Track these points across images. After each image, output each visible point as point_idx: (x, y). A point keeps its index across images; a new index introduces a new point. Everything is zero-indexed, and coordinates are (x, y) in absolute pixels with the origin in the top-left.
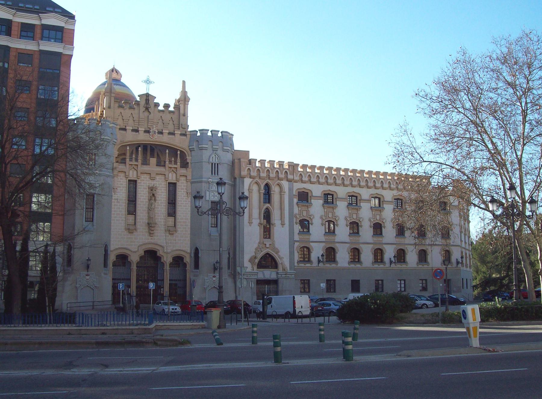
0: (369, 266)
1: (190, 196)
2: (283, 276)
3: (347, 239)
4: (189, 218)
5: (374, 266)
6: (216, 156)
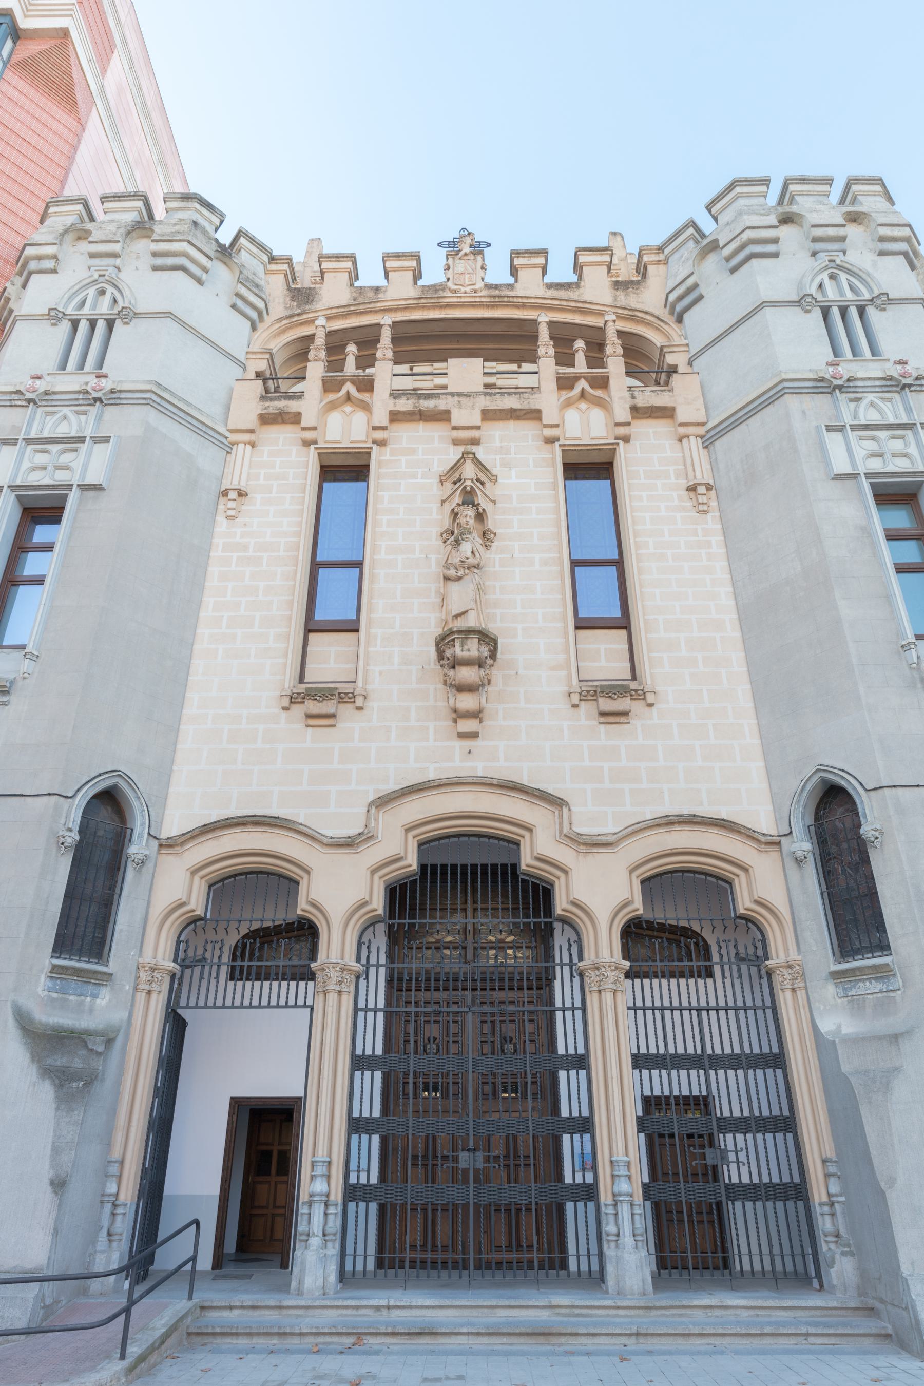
1: (714, 504)
6: (843, 277)
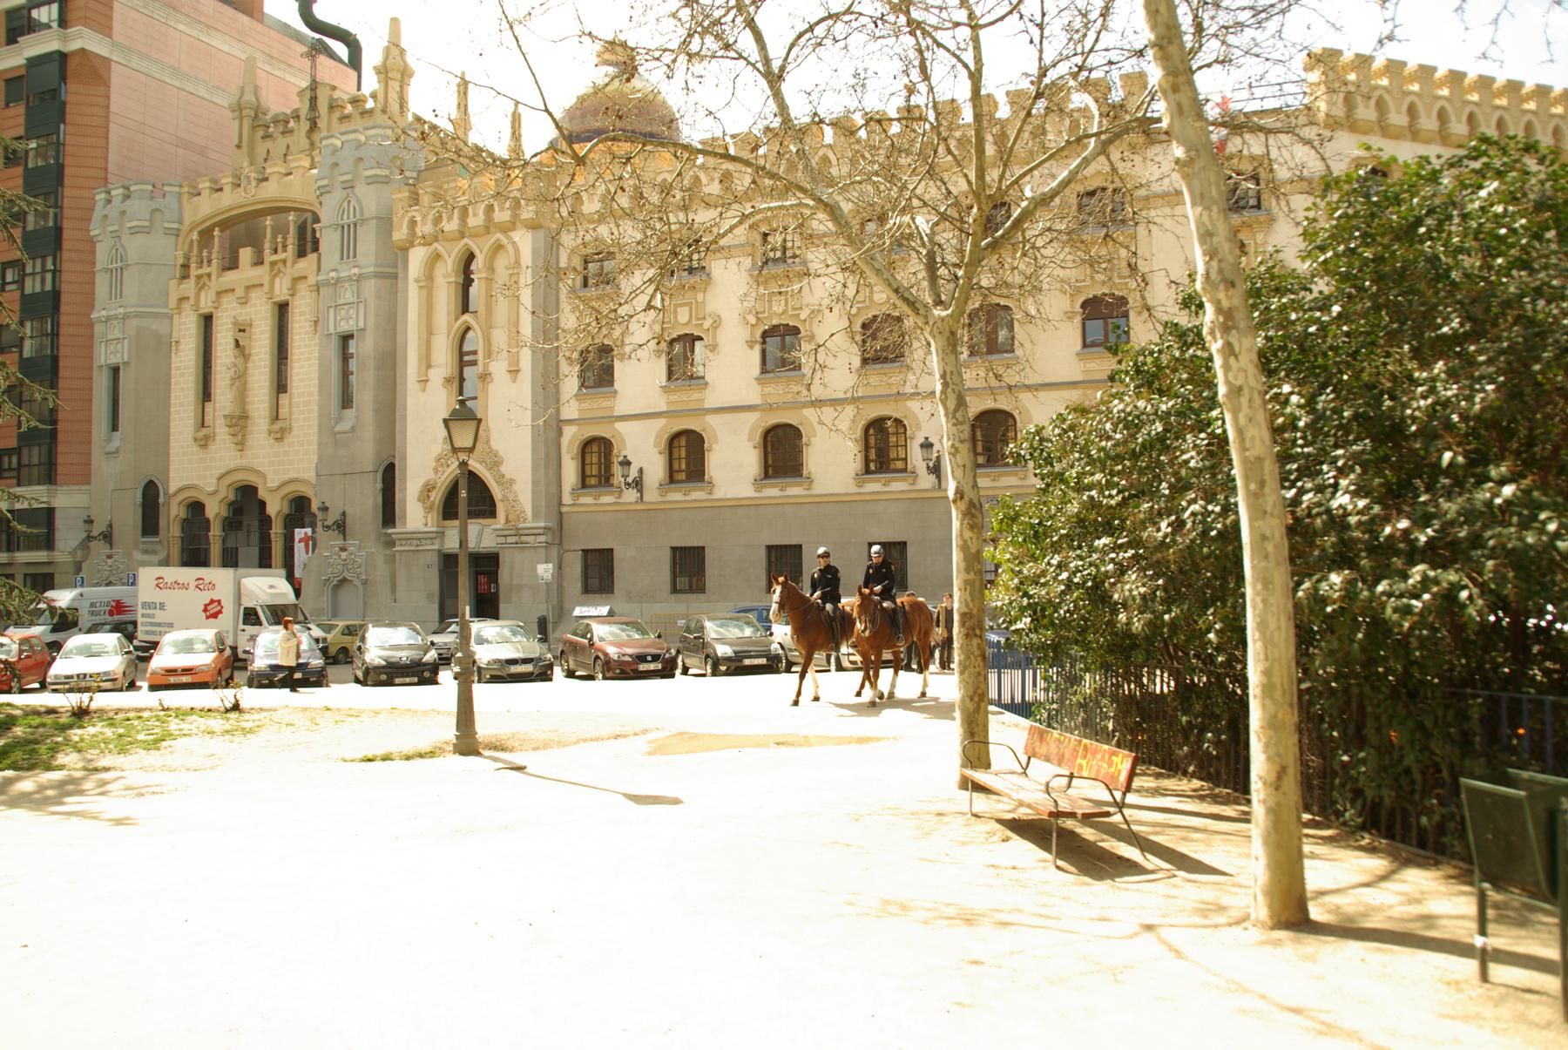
0: (839, 488)
2: (510, 540)
3: (750, 393)
4: (316, 390)
5: (862, 490)
